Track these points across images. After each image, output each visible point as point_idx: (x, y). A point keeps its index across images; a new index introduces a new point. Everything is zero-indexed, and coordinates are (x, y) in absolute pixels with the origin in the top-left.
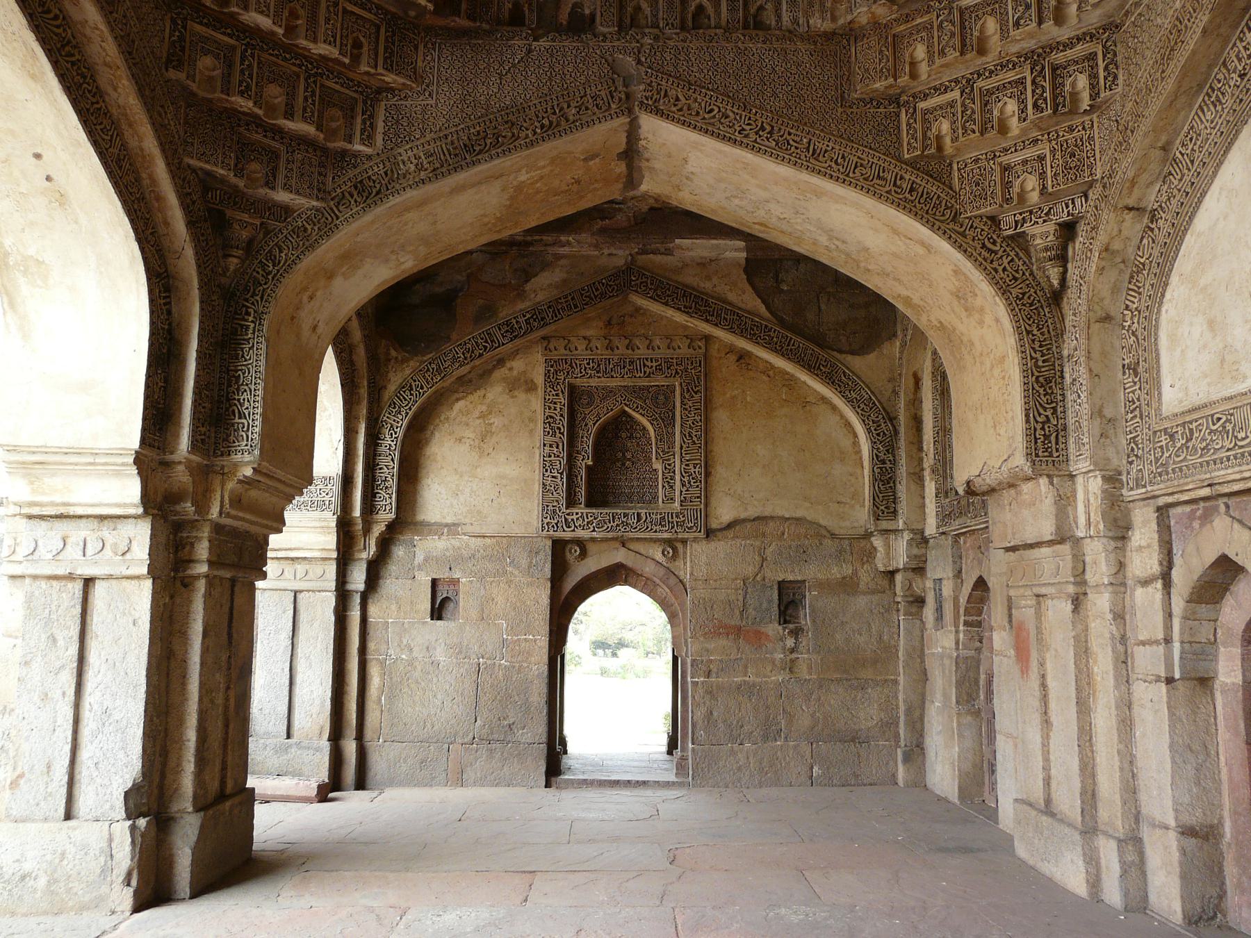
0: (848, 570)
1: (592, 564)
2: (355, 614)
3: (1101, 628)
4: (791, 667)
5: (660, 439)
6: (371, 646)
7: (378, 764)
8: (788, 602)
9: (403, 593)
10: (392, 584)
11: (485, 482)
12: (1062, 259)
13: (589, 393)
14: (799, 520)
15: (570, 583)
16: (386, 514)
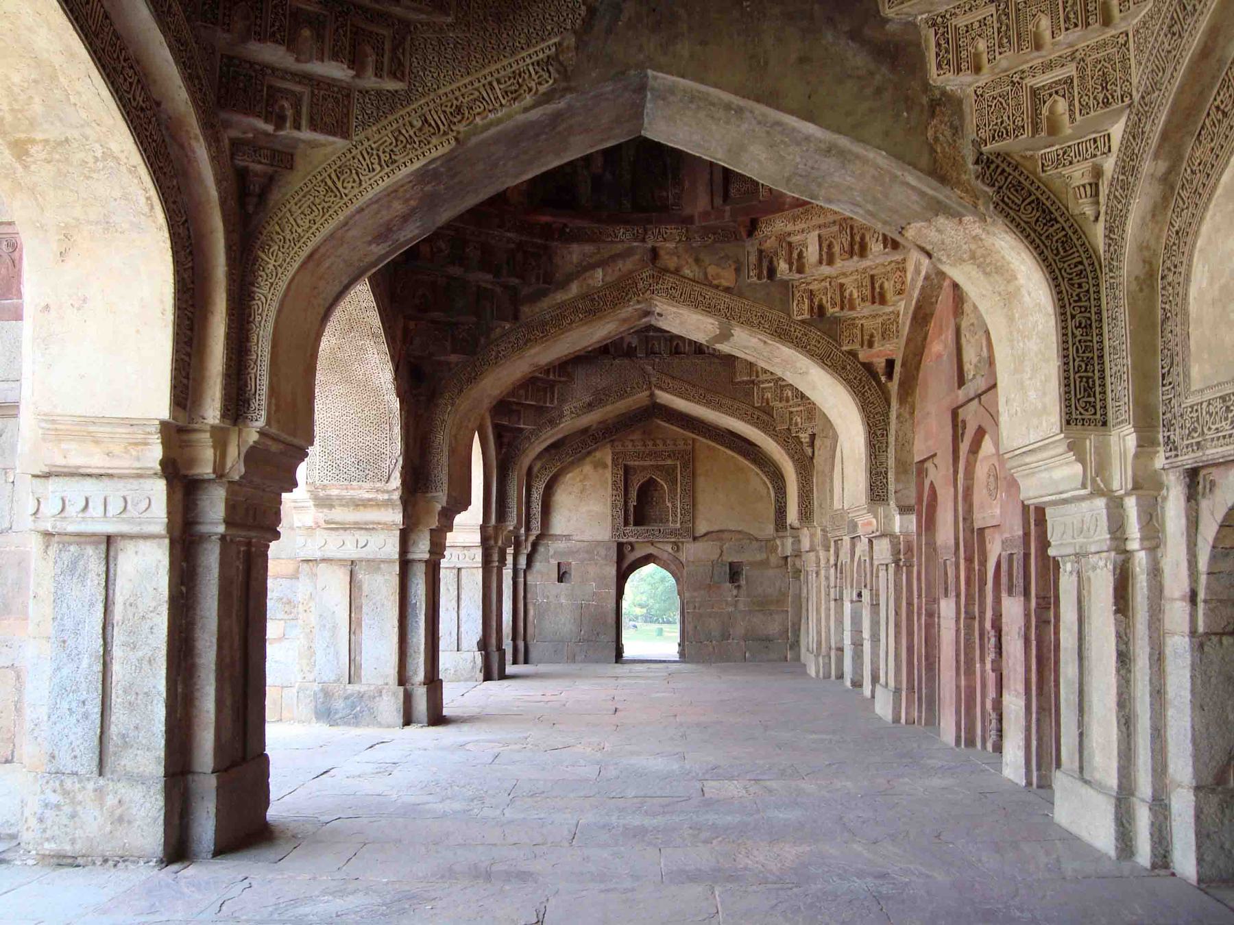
0: (764, 556)
1: (638, 554)
2: (521, 580)
3: (823, 583)
4: (736, 604)
5: (670, 491)
6: (529, 596)
7: (533, 654)
8: (734, 573)
9: (544, 569)
10: (538, 565)
11: (583, 513)
12: (812, 444)
13: (634, 468)
14: (740, 532)
15: (625, 564)
16: (536, 532)
